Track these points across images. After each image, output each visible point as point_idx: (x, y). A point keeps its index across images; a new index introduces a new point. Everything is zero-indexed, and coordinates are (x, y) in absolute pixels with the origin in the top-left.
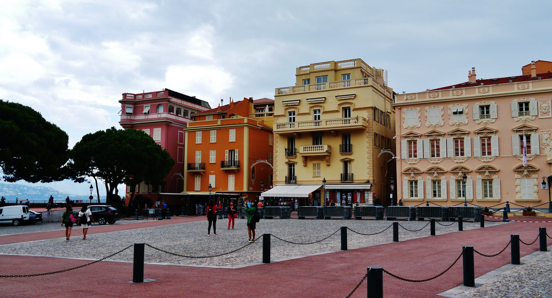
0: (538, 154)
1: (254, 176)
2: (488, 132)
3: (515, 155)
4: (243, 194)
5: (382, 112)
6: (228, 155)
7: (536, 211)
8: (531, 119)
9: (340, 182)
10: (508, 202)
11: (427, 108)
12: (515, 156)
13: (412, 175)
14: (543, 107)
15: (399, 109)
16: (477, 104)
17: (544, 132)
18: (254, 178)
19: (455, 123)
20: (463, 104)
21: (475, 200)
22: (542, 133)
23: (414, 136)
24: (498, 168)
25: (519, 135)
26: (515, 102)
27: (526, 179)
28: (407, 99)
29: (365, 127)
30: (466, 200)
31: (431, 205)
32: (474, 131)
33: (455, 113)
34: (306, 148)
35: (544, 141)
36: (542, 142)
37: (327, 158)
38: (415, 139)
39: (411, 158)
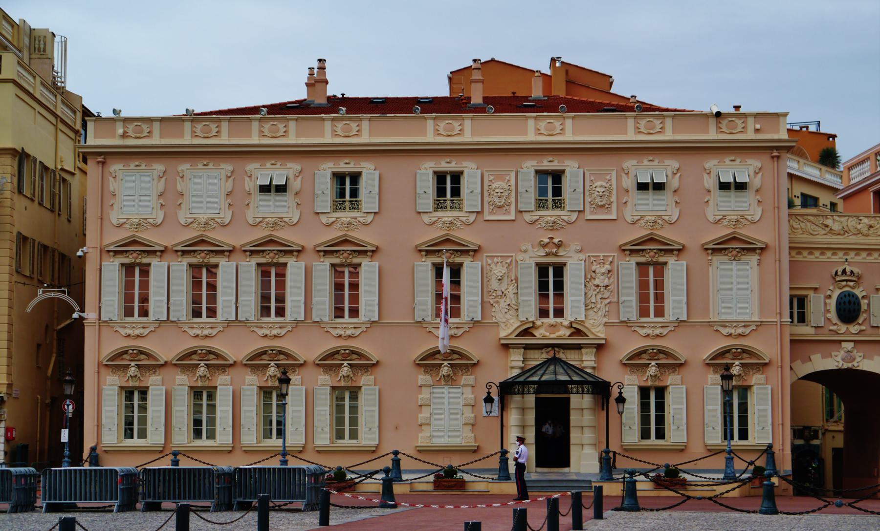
0: (478, 318)
2: (351, 251)
3: (420, 320)
5: (46, 168)
7: (467, 477)
8: (464, 219)
10: (396, 453)
11: (184, 167)
12: (421, 323)
13: (133, 371)
14: (497, 191)
15: (100, 165)
16: (327, 169)
17: (496, 260)
19: (264, 218)
20: (289, 165)
21: (310, 447)
22: (490, 261)
24: (374, 355)
25: (434, 264)
26: (427, 169)
27: (446, 388)
28: (124, 136)
30: (284, 447)
31: (185, 464)
32: (316, 246)
33: (265, 189)
35: (494, 284)
36: (490, 287)
38: (145, 260)
39: (129, 319)
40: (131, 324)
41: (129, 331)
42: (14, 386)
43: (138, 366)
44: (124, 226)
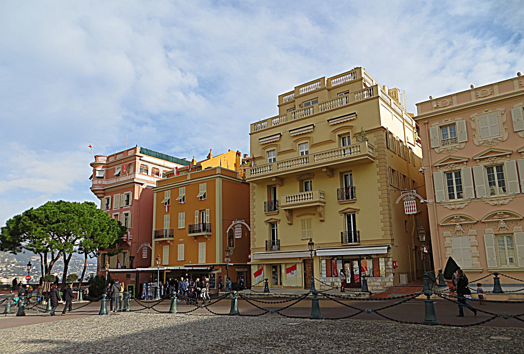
1: (233, 244)
4: (215, 268)
6: (198, 217)
9: (341, 245)
18: (233, 246)
23: (456, 163)
29: (374, 158)
34: (289, 197)
37: (320, 209)
38: (457, 168)
40: (454, 203)
41: (453, 207)
42: (394, 240)
43: (461, 225)
44: (443, 152)
